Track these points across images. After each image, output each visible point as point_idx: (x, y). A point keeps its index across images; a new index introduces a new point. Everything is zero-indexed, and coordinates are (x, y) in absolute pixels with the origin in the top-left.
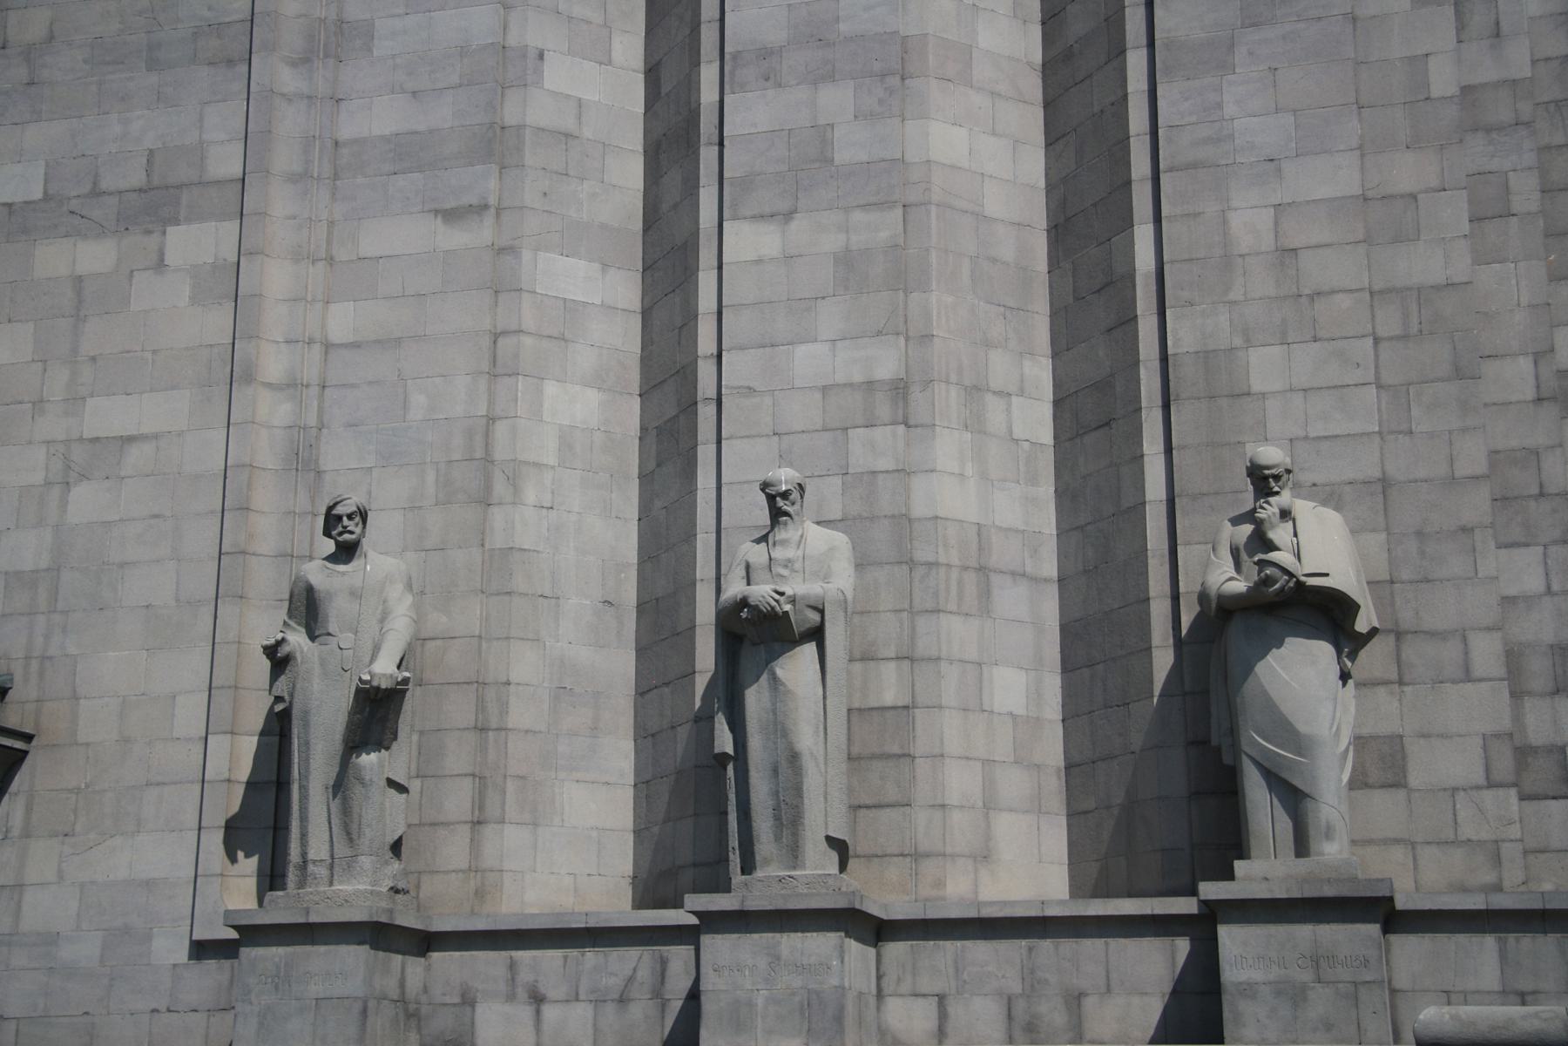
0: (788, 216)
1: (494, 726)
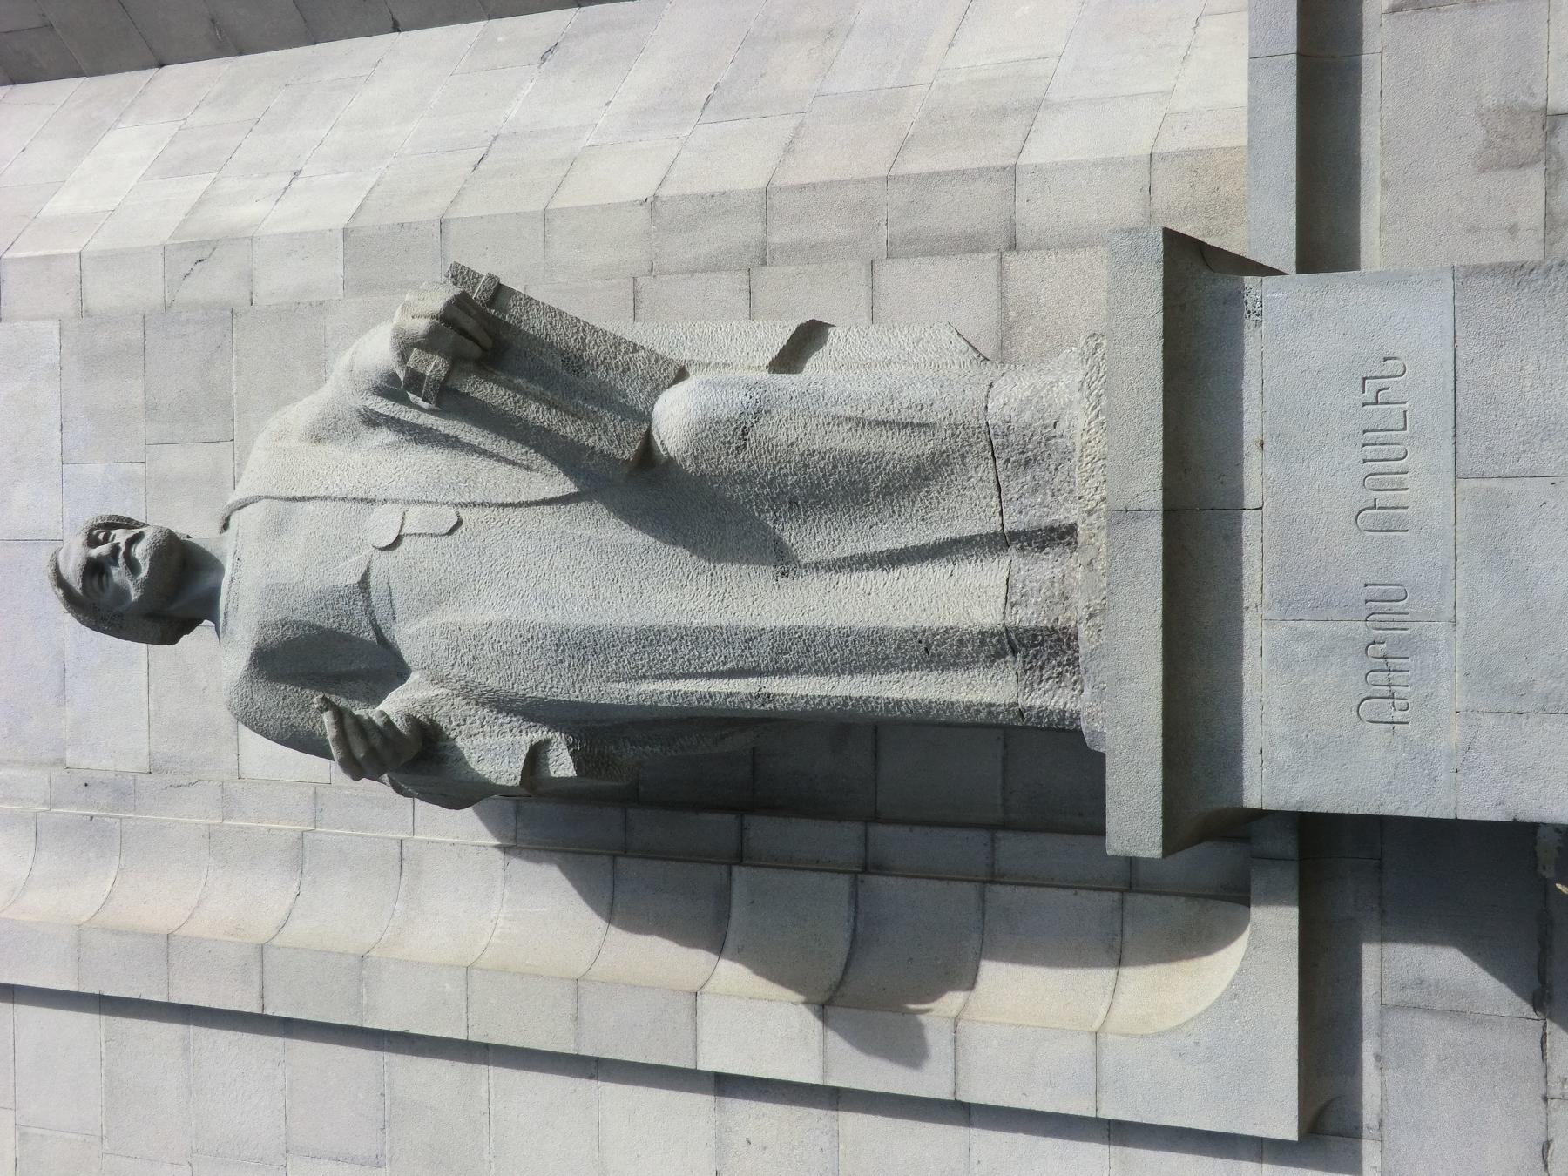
1: (756, 229)
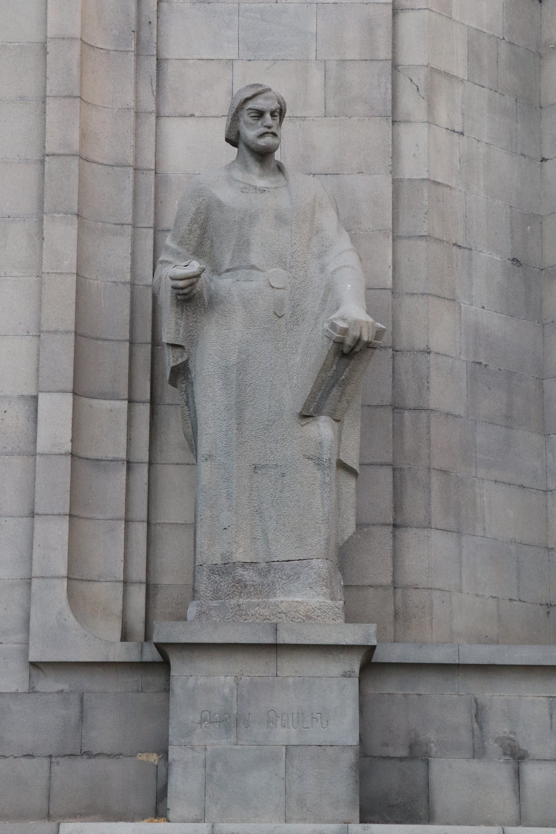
1: (412, 405)
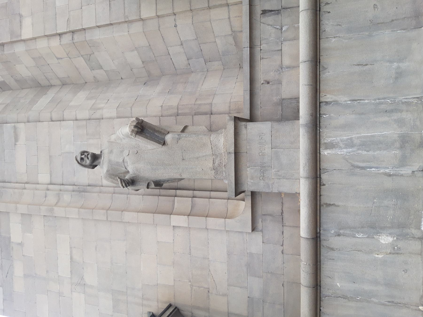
0: (21, 16)
1: (176, 110)
